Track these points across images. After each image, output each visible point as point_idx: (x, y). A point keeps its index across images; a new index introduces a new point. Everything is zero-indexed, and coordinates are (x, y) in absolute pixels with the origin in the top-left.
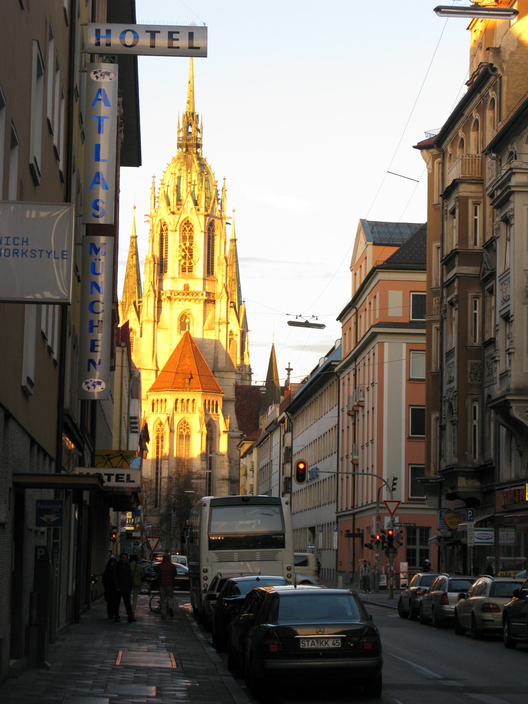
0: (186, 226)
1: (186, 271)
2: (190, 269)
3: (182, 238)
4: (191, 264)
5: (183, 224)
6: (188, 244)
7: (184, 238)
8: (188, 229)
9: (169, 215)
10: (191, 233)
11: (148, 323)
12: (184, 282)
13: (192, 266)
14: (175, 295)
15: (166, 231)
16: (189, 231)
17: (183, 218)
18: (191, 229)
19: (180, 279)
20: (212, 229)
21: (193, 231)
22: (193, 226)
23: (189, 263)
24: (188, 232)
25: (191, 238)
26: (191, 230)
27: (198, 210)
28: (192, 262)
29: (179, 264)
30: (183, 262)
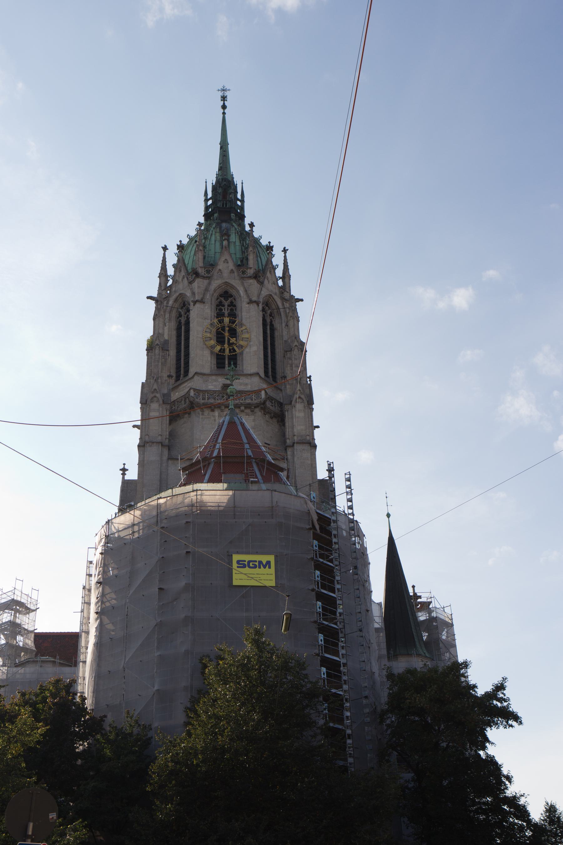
0: (222, 299)
1: (224, 367)
2: (234, 359)
3: (216, 315)
4: (235, 351)
5: (216, 295)
6: (226, 320)
7: (220, 315)
8: (226, 303)
9: (190, 283)
10: (232, 310)
11: (151, 446)
12: (221, 381)
13: (236, 355)
14: (204, 399)
15: (186, 314)
16: (229, 306)
17: (216, 283)
18: (232, 302)
19: (214, 377)
20: (269, 312)
21: (235, 306)
22: (235, 299)
23: (230, 350)
24: (226, 306)
25: (233, 315)
26: (232, 305)
27: (243, 272)
28: (235, 347)
29: (212, 353)
30: (218, 348)
